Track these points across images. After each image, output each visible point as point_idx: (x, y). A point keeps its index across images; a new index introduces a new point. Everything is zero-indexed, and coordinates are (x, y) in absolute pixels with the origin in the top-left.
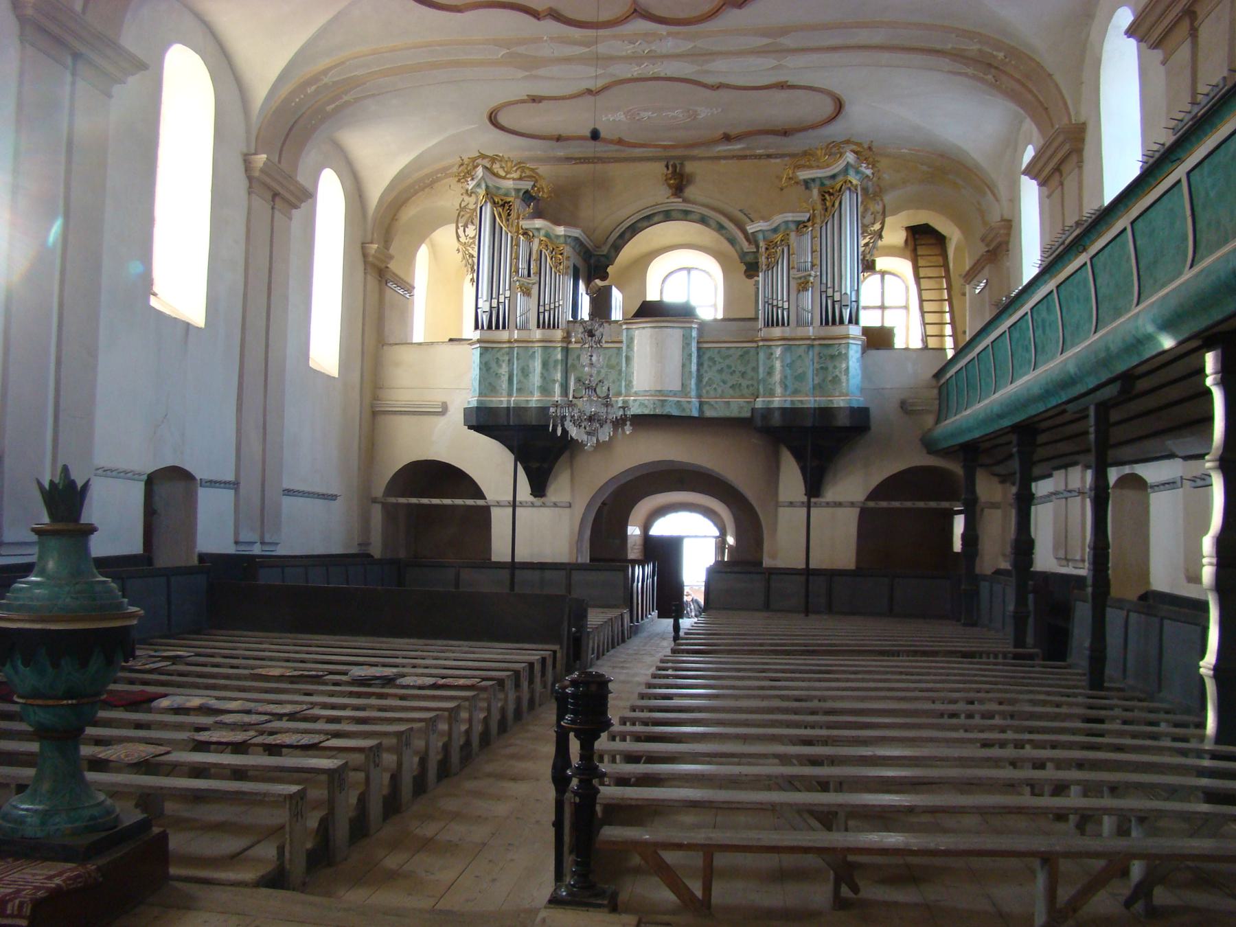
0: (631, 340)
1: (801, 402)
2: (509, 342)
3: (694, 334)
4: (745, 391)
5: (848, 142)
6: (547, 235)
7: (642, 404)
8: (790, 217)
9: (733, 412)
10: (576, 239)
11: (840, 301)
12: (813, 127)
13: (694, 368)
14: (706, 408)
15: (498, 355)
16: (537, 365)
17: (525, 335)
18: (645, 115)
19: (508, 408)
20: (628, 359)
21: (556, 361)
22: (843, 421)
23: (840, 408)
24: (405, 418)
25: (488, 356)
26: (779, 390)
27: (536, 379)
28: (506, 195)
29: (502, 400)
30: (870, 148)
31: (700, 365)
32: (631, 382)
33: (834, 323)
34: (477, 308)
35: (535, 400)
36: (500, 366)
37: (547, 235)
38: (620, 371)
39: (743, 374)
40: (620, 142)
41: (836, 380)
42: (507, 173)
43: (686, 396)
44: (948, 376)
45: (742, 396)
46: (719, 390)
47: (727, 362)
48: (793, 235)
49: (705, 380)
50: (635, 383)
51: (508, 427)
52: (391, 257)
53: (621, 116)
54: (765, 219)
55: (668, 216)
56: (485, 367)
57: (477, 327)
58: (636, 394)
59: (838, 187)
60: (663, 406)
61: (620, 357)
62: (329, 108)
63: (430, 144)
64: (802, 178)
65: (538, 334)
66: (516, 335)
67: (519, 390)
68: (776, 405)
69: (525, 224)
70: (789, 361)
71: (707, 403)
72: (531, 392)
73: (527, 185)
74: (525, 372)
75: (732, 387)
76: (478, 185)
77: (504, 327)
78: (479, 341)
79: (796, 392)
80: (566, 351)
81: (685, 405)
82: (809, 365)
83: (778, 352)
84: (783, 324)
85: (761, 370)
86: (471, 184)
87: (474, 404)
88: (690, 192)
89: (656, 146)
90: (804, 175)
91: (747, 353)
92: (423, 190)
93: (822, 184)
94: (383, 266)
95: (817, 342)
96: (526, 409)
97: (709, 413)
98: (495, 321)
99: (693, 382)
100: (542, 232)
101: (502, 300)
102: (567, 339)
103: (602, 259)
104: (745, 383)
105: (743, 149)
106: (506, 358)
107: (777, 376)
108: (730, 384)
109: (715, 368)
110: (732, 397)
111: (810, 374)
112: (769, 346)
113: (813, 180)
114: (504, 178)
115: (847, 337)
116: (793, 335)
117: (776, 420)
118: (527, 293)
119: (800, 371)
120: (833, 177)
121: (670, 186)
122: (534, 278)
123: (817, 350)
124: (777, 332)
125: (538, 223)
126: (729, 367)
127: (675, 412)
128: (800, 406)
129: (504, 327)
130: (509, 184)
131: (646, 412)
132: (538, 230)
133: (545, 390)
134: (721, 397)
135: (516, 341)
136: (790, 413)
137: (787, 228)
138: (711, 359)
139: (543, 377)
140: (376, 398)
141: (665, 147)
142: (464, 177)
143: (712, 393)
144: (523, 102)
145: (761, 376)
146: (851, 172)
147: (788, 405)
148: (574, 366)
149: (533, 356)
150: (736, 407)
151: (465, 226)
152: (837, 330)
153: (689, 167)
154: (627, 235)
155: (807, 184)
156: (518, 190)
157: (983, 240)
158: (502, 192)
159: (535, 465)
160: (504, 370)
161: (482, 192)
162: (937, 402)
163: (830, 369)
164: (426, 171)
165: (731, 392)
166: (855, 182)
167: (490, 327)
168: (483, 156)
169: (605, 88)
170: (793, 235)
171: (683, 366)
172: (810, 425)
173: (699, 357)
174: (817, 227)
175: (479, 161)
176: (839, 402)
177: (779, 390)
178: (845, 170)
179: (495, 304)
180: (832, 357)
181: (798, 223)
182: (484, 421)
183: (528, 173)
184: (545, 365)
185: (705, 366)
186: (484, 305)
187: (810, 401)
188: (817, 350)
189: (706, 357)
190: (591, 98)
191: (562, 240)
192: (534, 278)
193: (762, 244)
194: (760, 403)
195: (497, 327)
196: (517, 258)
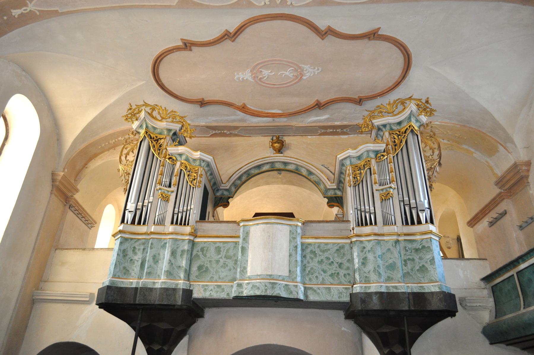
0: (247, 234)
1: (396, 287)
2: (145, 234)
3: (299, 231)
4: (343, 279)
5: (410, 98)
6: (187, 160)
7: (254, 286)
8: (372, 146)
9: (335, 298)
10: (208, 165)
11: (417, 207)
12: (382, 94)
13: (299, 258)
14: (309, 292)
15: (136, 245)
16: (167, 254)
17: (159, 229)
18: (266, 73)
19: (136, 289)
20: (244, 249)
21: (183, 251)
22: (436, 305)
23: (432, 293)
24: (59, 306)
25: (126, 245)
26: (373, 277)
27: (164, 265)
28: (160, 134)
29: (132, 282)
30: (427, 102)
31: (304, 256)
32: (245, 268)
33: (413, 223)
34: (125, 209)
35: (160, 282)
36: (135, 253)
37: (187, 160)
38: (236, 261)
39: (340, 265)
40: (244, 109)
41: (423, 269)
42: (163, 118)
43: (294, 280)
44: (522, 266)
45: (340, 284)
46: (320, 278)
47: (326, 254)
48: (373, 162)
49: (308, 269)
50: (249, 269)
51: (135, 307)
52: (77, 191)
53: (247, 75)
54: (355, 148)
55: (273, 168)
56: (123, 254)
57: (123, 221)
58: (250, 278)
59: (403, 130)
60: (273, 288)
61: (234, 254)
62: (16, 12)
63: (112, 100)
64: (376, 124)
65: (171, 228)
66: (153, 229)
67: (149, 274)
68: (373, 290)
69: (173, 150)
70: (379, 252)
71: (311, 288)
72: (160, 276)
73: (176, 127)
74: (156, 259)
75: (332, 275)
76: (141, 126)
77: (144, 224)
78: (120, 232)
79: (389, 279)
80: (193, 244)
81: (293, 289)
82: (396, 257)
83: (369, 246)
84: (371, 224)
85: (356, 261)
86: (135, 125)
87: (107, 283)
88: (288, 153)
89: (268, 115)
90: (377, 122)
91: (342, 247)
92: (108, 150)
93: (391, 129)
94: (70, 194)
95: (401, 238)
96: (151, 289)
97: (312, 298)
98: (139, 219)
99: (299, 269)
100: (184, 157)
101: (145, 204)
102: (194, 234)
103: (226, 193)
104: (342, 272)
105: (327, 120)
106: (142, 247)
107: (370, 267)
108: (329, 273)
109: (316, 260)
110: (332, 284)
111: (399, 264)
112: (361, 242)
113: (385, 126)
114: (160, 121)
115: (431, 232)
116: (381, 232)
117: (375, 304)
118: (166, 199)
119: (390, 261)
120: (399, 123)
121: (274, 148)
122: (174, 188)
123: (402, 244)
124: (367, 229)
125: (181, 149)
126: (328, 259)
127: (284, 294)
128: (395, 291)
129: (144, 224)
130: (162, 125)
131: (258, 293)
132: (181, 155)
133: (169, 274)
134: (322, 284)
135: (152, 233)
136: (388, 297)
137: (368, 156)
138: (312, 252)
139: (170, 263)
140: (37, 287)
141: (273, 116)
142: (131, 118)
143: (314, 281)
144: (177, 49)
145: (357, 266)
146: (413, 120)
147: (383, 290)
148: (197, 256)
149: (164, 246)
150: (338, 293)
151: (128, 154)
152: (416, 228)
153: (287, 140)
154: (244, 178)
155: (379, 129)
156: (169, 130)
157: (497, 183)
158: (158, 131)
159: (156, 347)
160: (138, 257)
161: (142, 132)
162: (492, 299)
163: (417, 260)
164: (110, 131)
165: (331, 280)
166: (416, 128)
167: (133, 222)
168: (146, 105)
169: (240, 30)
170: (373, 162)
171: (290, 255)
172: (406, 308)
173: (303, 250)
174: (391, 156)
175: (143, 108)
176: (431, 288)
177: (373, 277)
178: (409, 118)
179: (139, 207)
180: (417, 250)
181: (377, 152)
182: (115, 301)
183: (178, 119)
184: (173, 253)
185: (308, 257)
186: (131, 206)
187: (404, 287)
188: (402, 244)
189: (308, 250)
190: (228, 43)
191: (198, 163)
192: (174, 188)
193: (349, 170)
194: (357, 288)
195: (139, 223)
196: (162, 174)
